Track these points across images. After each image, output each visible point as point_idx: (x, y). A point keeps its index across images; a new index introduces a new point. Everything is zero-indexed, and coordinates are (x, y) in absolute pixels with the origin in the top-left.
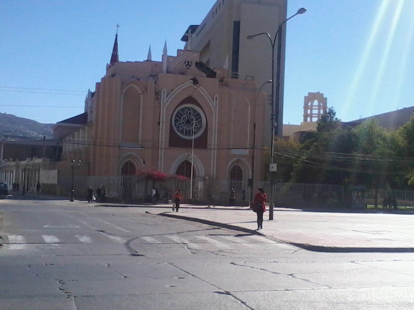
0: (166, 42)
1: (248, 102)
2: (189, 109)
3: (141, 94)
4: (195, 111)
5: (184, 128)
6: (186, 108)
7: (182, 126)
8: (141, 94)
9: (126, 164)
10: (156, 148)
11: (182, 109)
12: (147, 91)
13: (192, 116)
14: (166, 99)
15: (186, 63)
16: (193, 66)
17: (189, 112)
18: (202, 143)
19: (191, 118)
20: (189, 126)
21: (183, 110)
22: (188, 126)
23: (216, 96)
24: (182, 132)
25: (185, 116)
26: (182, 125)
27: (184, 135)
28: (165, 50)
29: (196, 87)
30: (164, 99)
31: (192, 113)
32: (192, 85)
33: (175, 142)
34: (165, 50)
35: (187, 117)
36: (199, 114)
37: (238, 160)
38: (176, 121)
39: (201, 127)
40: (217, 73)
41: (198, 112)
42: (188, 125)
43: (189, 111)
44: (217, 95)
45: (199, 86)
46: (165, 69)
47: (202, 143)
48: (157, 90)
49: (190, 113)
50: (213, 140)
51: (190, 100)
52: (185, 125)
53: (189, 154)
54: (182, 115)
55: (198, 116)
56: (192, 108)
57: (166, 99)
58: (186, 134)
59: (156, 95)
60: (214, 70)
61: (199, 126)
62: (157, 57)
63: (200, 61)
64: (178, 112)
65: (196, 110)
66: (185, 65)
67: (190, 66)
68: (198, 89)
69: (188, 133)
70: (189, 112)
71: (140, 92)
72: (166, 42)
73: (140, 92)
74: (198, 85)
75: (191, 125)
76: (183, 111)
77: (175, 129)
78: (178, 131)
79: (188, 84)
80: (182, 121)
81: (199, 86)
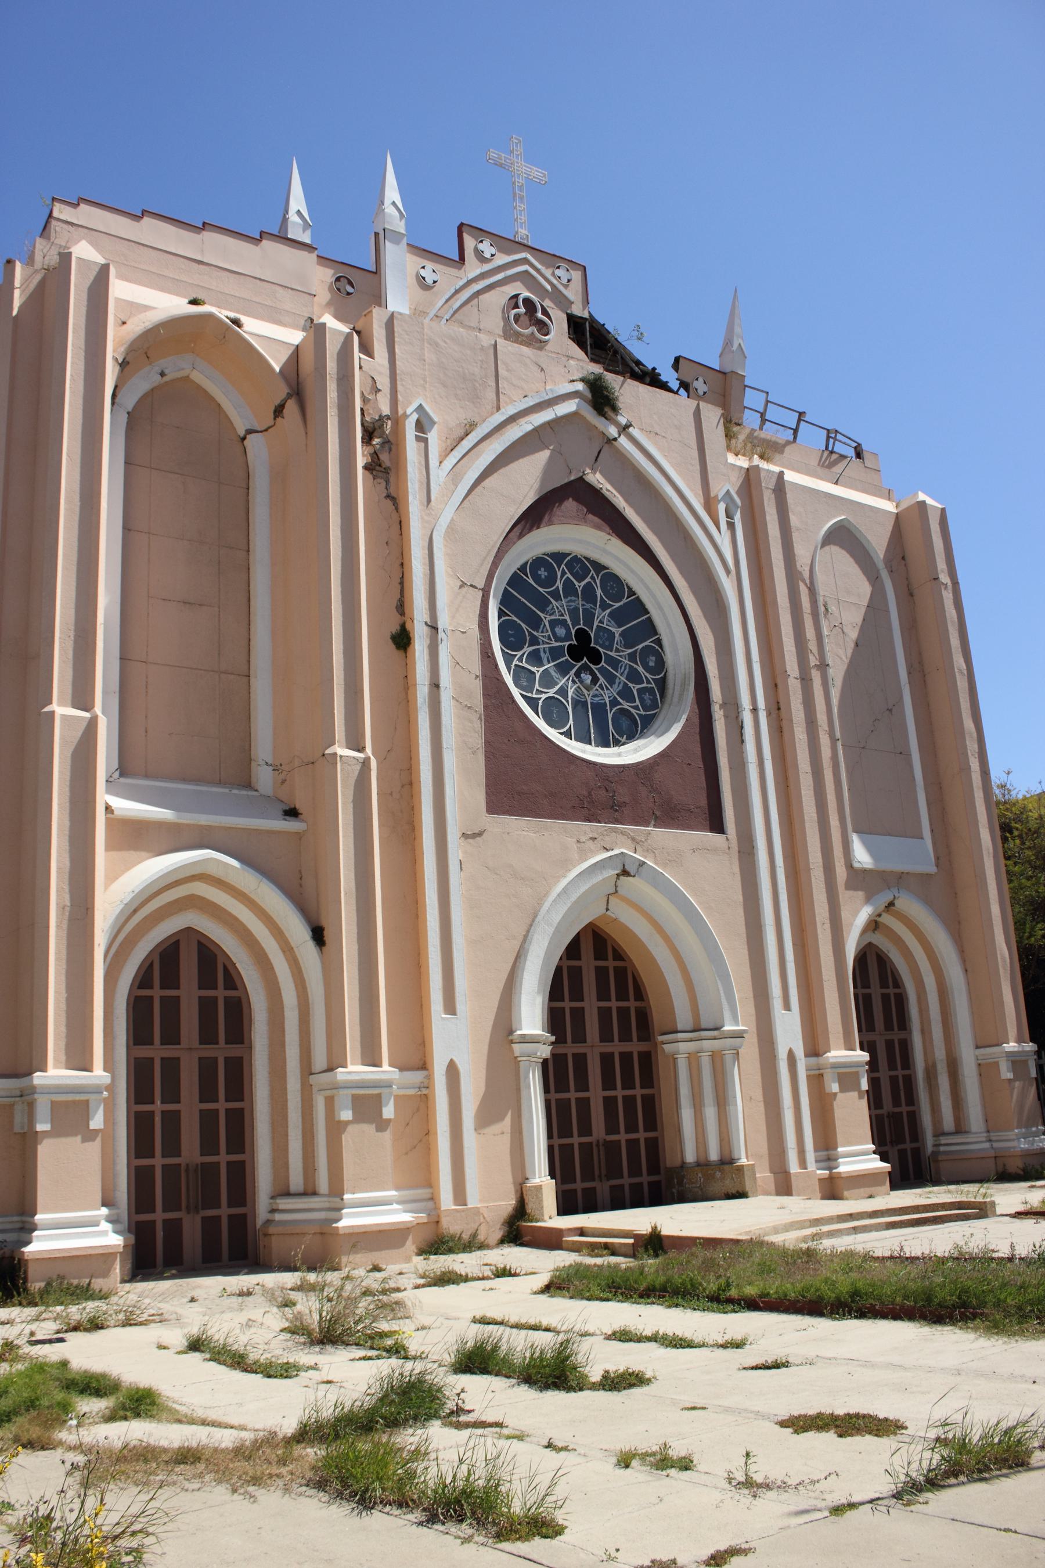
3: (250, 432)
5: (563, 691)
8: (250, 432)
11: (538, 562)
13: (602, 617)
17: (579, 586)
19: (596, 623)
20: (595, 680)
25: (560, 608)
31: (599, 592)
35: (575, 621)
36: (638, 607)
39: (662, 684)
41: (632, 593)
42: (585, 668)
49: (589, 593)
54: (543, 604)
61: (648, 682)
64: (515, 581)
70: (579, 586)
75: (602, 670)
76: (543, 573)
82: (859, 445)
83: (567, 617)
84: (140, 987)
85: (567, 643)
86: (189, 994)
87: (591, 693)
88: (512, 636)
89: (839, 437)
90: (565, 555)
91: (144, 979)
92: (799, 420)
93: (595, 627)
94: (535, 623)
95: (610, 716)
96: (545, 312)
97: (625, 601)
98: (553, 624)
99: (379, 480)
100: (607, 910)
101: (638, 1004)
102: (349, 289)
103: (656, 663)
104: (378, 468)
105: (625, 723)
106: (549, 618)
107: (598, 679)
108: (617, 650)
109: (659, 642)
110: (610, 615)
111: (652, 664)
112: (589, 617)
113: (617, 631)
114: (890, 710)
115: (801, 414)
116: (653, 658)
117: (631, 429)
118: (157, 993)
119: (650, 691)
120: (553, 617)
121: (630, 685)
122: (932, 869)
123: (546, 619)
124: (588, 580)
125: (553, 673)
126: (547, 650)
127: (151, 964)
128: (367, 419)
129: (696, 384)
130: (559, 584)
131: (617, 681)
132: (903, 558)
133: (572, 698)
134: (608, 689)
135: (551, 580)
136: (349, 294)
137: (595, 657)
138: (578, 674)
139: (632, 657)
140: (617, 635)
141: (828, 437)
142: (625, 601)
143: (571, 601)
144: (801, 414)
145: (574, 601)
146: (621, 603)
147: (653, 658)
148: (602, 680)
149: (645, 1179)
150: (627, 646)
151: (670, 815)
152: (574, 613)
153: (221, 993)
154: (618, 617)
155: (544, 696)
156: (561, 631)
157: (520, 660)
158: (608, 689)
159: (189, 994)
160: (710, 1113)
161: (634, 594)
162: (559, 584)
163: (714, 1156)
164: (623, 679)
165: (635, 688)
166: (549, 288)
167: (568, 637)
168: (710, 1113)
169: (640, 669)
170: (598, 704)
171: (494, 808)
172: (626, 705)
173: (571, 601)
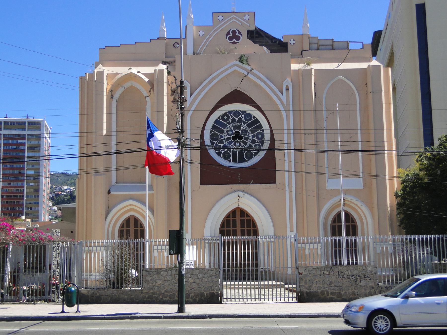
2: (237, 113)
4: (248, 116)
6: (230, 112)
7: (225, 145)
9: (127, 222)
11: (224, 115)
12: (153, 90)
13: (244, 127)
16: (244, 37)
17: (237, 119)
18: (265, 173)
21: (225, 116)
22: (238, 144)
24: (226, 156)
26: (226, 143)
27: (230, 161)
31: (243, 119)
33: (211, 174)
36: (257, 121)
38: (213, 137)
40: (289, 45)
41: (254, 117)
42: (237, 142)
43: (237, 117)
47: (265, 173)
51: (237, 96)
54: (225, 126)
55: (255, 124)
56: (243, 112)
58: (234, 160)
59: (171, 95)
60: (282, 40)
63: (256, 28)
65: (249, 114)
68: (250, 76)
69: (238, 157)
70: (237, 119)
71: (145, 94)
73: (145, 94)
75: (243, 142)
76: (225, 118)
77: (212, 152)
78: (219, 154)
79: (230, 67)
83: (232, 129)
84: (122, 228)
86: (132, 229)
90: (232, 111)
91: (122, 226)
94: (222, 132)
95: (244, 154)
96: (239, 33)
98: (227, 131)
101: (254, 228)
102: (177, 46)
108: (248, 135)
111: (260, 137)
112: (239, 127)
113: (249, 130)
117: (253, 71)
118: (125, 229)
122: (362, 188)
124: (240, 116)
127: (124, 223)
129: (290, 42)
130: (230, 120)
132: (366, 84)
139: (253, 136)
140: (248, 131)
142: (252, 120)
152: (234, 127)
153: (139, 228)
154: (249, 126)
155: (223, 152)
157: (217, 143)
159: (132, 229)
166: (241, 24)
169: (256, 139)
171: (202, 183)
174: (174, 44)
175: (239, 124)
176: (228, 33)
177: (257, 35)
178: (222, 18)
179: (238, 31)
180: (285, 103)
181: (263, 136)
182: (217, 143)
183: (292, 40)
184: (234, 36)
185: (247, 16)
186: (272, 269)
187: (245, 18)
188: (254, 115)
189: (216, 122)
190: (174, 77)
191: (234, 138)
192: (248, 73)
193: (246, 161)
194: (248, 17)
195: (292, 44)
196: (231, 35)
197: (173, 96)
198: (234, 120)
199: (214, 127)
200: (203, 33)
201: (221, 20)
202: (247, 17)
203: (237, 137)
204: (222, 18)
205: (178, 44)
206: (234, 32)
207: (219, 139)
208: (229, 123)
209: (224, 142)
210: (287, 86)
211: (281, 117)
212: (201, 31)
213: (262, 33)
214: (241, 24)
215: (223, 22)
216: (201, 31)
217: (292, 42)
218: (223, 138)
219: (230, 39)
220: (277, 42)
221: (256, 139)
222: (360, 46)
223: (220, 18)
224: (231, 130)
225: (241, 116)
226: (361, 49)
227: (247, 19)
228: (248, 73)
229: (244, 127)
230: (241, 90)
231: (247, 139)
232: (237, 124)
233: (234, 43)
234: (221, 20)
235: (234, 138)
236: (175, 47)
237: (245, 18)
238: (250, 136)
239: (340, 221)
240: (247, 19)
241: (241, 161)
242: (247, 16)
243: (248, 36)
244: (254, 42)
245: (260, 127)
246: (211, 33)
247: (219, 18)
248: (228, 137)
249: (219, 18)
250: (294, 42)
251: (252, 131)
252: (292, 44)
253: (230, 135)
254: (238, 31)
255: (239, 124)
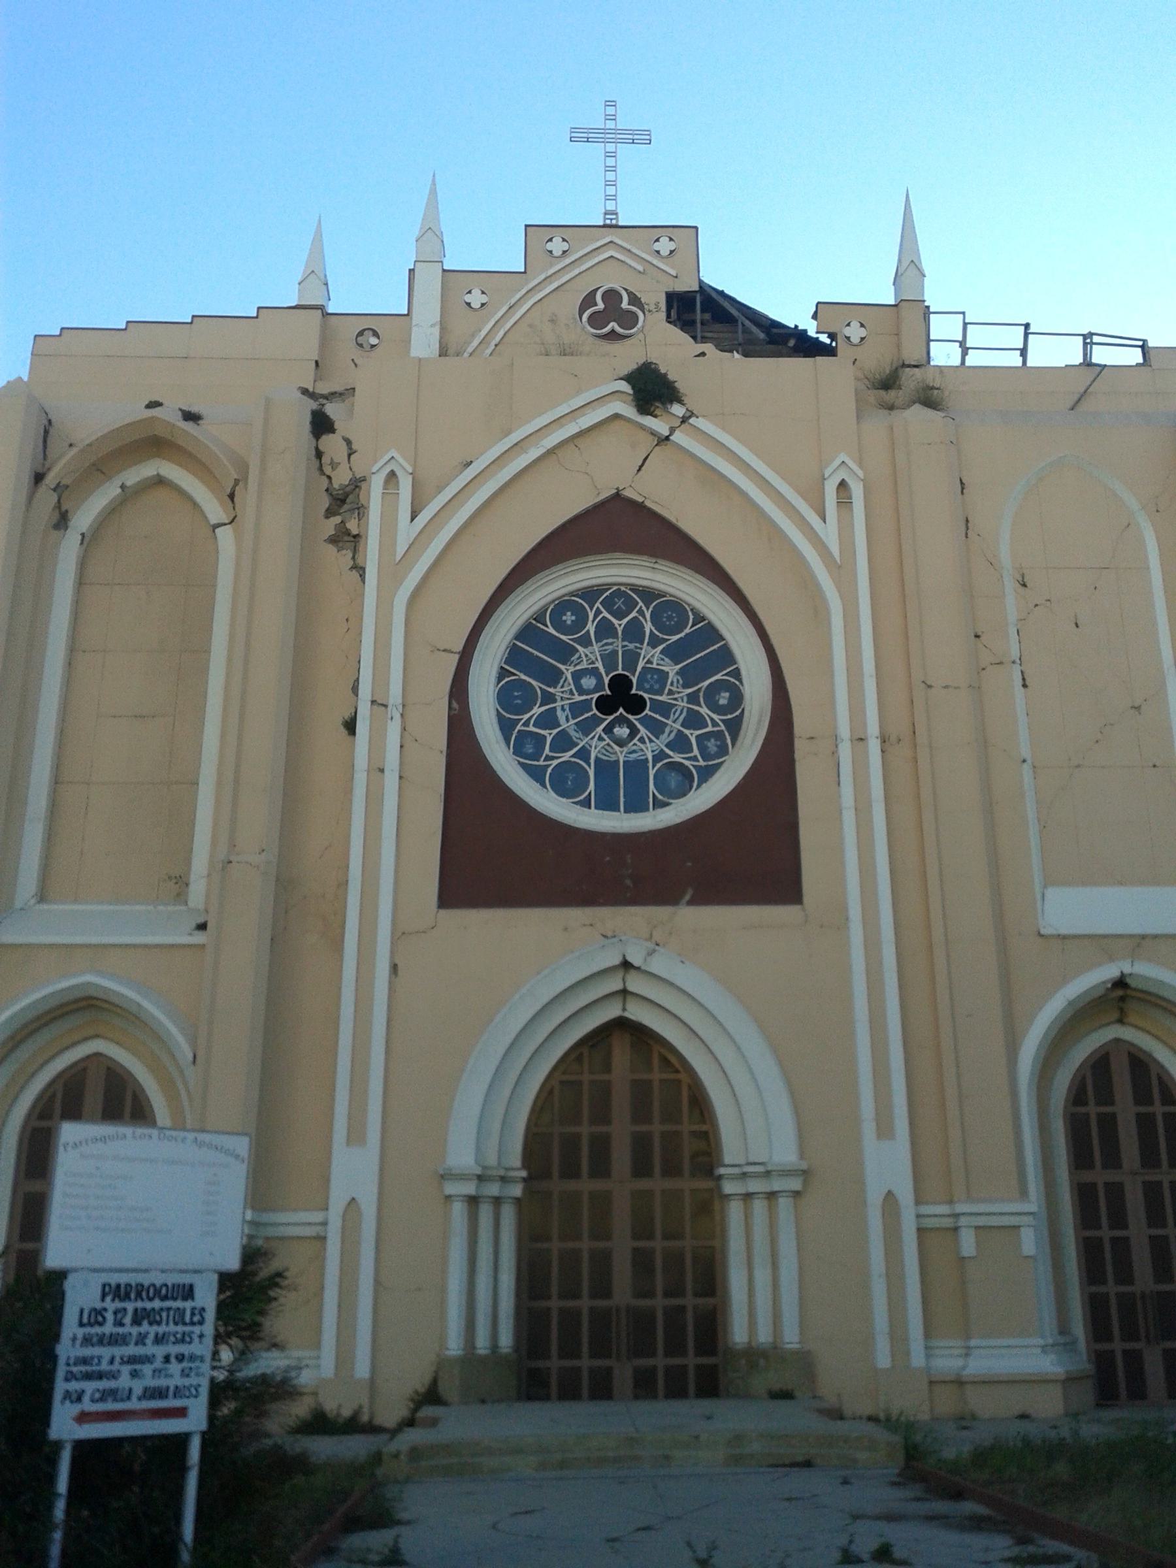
0: (433, 192)
1: (1133, 504)
2: (619, 599)
4: (671, 612)
5: (584, 754)
6: (590, 594)
7: (563, 732)
10: (297, 907)
11: (562, 605)
14: (406, 531)
15: (613, 331)
17: (620, 624)
22: (622, 732)
23: (842, 475)
24: (565, 783)
25: (591, 655)
26: (567, 723)
27: (586, 803)
28: (430, 233)
29: (660, 426)
30: (386, 522)
31: (648, 627)
32: (629, 411)
34: (430, 233)
36: (710, 633)
37: (1121, 983)
39: (735, 727)
41: (699, 618)
42: (621, 721)
44: (841, 465)
45: (684, 420)
46: (424, 341)
48: (341, 478)
49: (634, 632)
50: (846, 824)
51: (620, 524)
52: (596, 721)
53: (636, 960)
54: (565, 653)
55: (703, 651)
56: (648, 595)
57: (406, 531)
58: (607, 803)
59: (329, 513)
62: (369, 285)
66: (585, 316)
67: (629, 320)
68: (677, 437)
69: (621, 786)
70: (620, 624)
72: (433, 192)
74: (678, 410)
76: (569, 618)
78: (536, 774)
80: (564, 694)
81: (684, 420)
82: (1144, 341)
85: (596, 696)
87: (625, 749)
88: (517, 697)
89: (1096, 339)
92: (1026, 335)
93: (639, 669)
97: (687, 631)
98: (577, 676)
99: (344, 552)
100: (624, 1009)
102: (374, 341)
103: (730, 698)
104: (346, 538)
105: (673, 780)
106: (572, 669)
107: (639, 731)
108: (671, 692)
109: (737, 674)
110: (662, 652)
112: (631, 659)
113: (672, 670)
114: (1137, 708)
115: (1027, 326)
116: (727, 695)
117: (692, 421)
119: (719, 735)
120: (578, 667)
121: (687, 732)
123: (568, 671)
125: (573, 733)
126: (567, 708)
128: (336, 486)
129: (847, 331)
130: (591, 627)
131: (667, 730)
133: (597, 759)
134: (651, 741)
135: (582, 621)
136: (373, 346)
137: (636, 705)
138: (608, 730)
140: (671, 675)
141: (1085, 344)
142: (687, 631)
143: (607, 644)
144: (1027, 326)
145: (611, 644)
146: (682, 635)
147: (727, 695)
148: (643, 731)
149: (691, 1360)
150: (685, 686)
151: (718, 887)
152: (609, 660)
154: (674, 653)
155: (555, 763)
156: (588, 682)
157: (526, 724)
158: (651, 741)
160: (762, 1276)
161: (703, 619)
162: (591, 627)
163: (764, 1336)
164: (678, 726)
165: (692, 735)
167: (599, 686)
168: (762, 1276)
169: (704, 710)
170: (637, 761)
172: (677, 758)
173: (607, 644)
174: (361, 333)
175: (631, 646)
176: (589, 300)
177: (707, 316)
178: (565, 246)
179: (630, 293)
180: (835, 550)
181: (737, 698)
182: (526, 724)
183: (855, 324)
184: (611, 314)
185: (664, 240)
186: (791, 1338)
187: (657, 246)
188: (697, 605)
189: (527, 632)
190: (348, 442)
191: (605, 705)
192: (672, 430)
193: (659, 805)
194: (672, 246)
195: (855, 340)
196: (601, 305)
197: (337, 519)
198: (606, 629)
199: (515, 656)
200: (484, 299)
201: (557, 253)
202: (665, 246)
203: (621, 698)
204: (565, 246)
205: (376, 334)
206: (612, 296)
207: (537, 710)
208: (585, 641)
209: (562, 720)
210: (843, 484)
211: (818, 610)
212: (476, 292)
213: (726, 305)
214: (640, 268)
215: (568, 261)
216: (476, 292)
217: (855, 332)
218: (559, 704)
219: (597, 320)
220: (792, 343)
221: (704, 710)
222: (1134, 357)
223: (557, 246)
224: (594, 672)
225: (641, 612)
226: (1138, 365)
227: (665, 253)
228: (672, 430)
229: (651, 656)
230: (640, 500)
231: (665, 709)
232: (619, 645)
233: (613, 336)
234: (557, 253)
235: (605, 705)
236: (361, 346)
237: (657, 246)
238: (678, 696)
239: (1106, 1095)
240: (665, 253)
241: (637, 805)
242: (664, 240)
243: (668, 316)
244: (694, 338)
245: (726, 657)
246: (518, 296)
247: (549, 246)
248: (578, 698)
249: (549, 246)
250: (863, 332)
251: (689, 677)
252: (855, 340)
253: (588, 692)
254: (630, 293)
255: (631, 646)
